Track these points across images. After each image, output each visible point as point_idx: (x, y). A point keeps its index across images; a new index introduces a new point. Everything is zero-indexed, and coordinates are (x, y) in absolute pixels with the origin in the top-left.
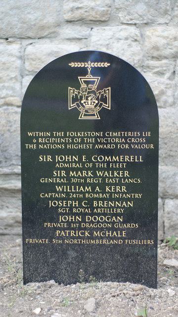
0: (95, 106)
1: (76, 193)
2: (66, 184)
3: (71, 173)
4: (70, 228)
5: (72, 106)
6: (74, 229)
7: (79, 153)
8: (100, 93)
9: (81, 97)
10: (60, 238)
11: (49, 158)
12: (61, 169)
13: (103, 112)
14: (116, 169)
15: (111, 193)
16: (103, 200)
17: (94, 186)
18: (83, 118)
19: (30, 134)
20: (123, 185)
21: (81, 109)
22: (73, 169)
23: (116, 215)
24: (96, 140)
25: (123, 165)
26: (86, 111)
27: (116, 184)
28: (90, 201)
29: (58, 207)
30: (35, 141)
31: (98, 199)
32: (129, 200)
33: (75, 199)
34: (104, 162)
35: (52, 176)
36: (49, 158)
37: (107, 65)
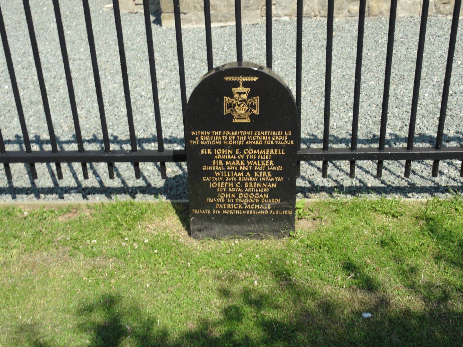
0: (247, 111)
1: (231, 177)
2: (223, 171)
3: (227, 162)
4: (226, 202)
5: (227, 111)
6: (231, 203)
7: (234, 147)
8: (250, 101)
9: (235, 105)
10: (218, 209)
11: (209, 152)
12: (218, 160)
13: (252, 116)
14: (263, 160)
15: (259, 178)
16: (253, 182)
17: (245, 172)
18: (237, 121)
19: (193, 133)
20: (269, 171)
21: (235, 115)
22: (229, 160)
23: (263, 193)
24: (247, 138)
25: (269, 157)
26: (238, 115)
27: (262, 171)
28: (243, 183)
29: (217, 188)
30: (197, 138)
31: (248, 182)
32: (274, 182)
33: (230, 182)
34: (253, 154)
35: (211, 164)
36: (209, 152)
37: (255, 79)
